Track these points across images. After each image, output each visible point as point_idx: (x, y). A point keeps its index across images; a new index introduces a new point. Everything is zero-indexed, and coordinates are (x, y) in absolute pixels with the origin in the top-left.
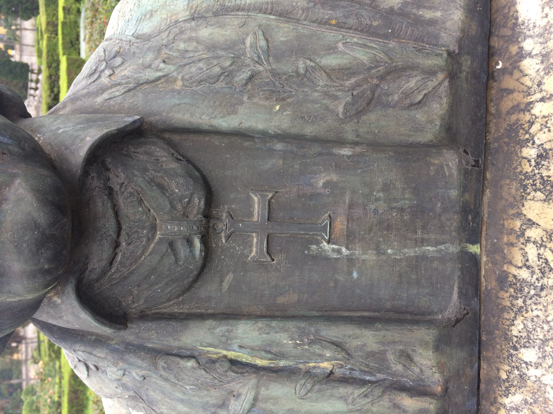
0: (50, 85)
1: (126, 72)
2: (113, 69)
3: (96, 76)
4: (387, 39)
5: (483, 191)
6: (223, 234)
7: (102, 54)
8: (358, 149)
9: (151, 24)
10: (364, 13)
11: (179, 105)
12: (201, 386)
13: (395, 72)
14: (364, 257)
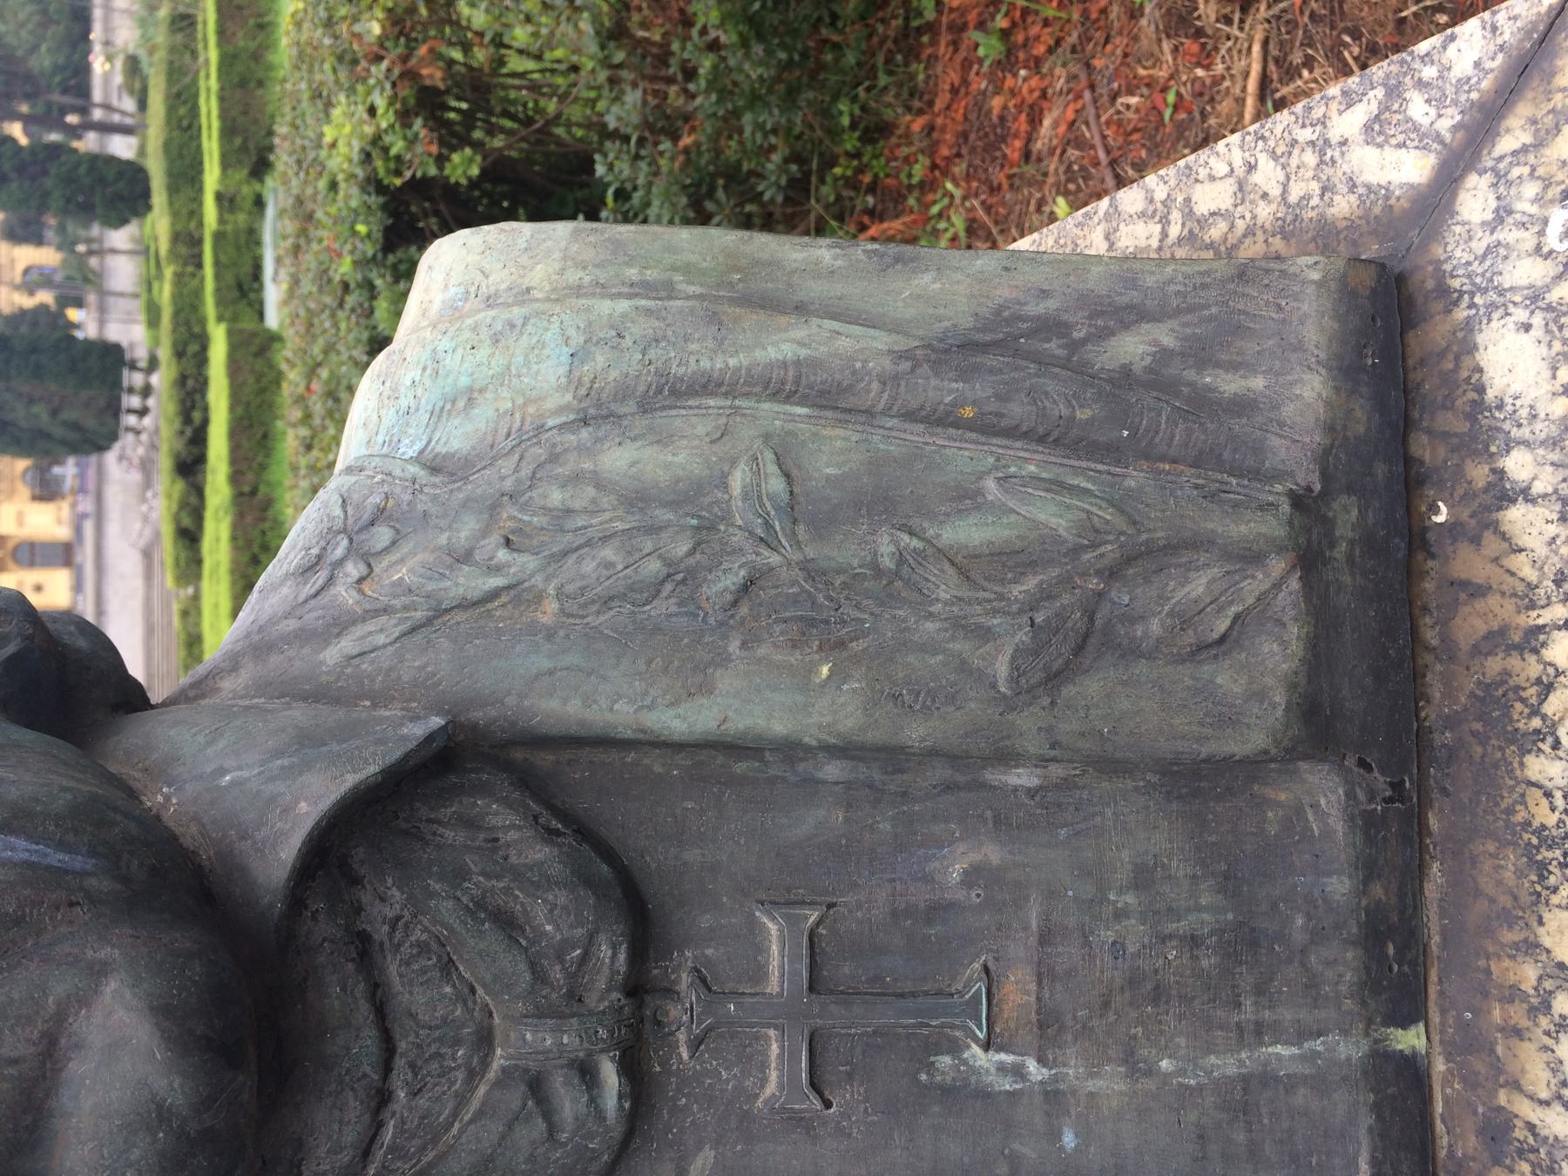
0: (182, 402)
1: (401, 573)
2: (368, 559)
3: (321, 577)
4: (1118, 463)
5: (1422, 871)
6: (682, 1036)
7: (338, 512)
8: (1057, 771)
9: (469, 428)
10: (1051, 386)
11: (551, 673)
13: (1147, 557)
14: (1092, 1085)
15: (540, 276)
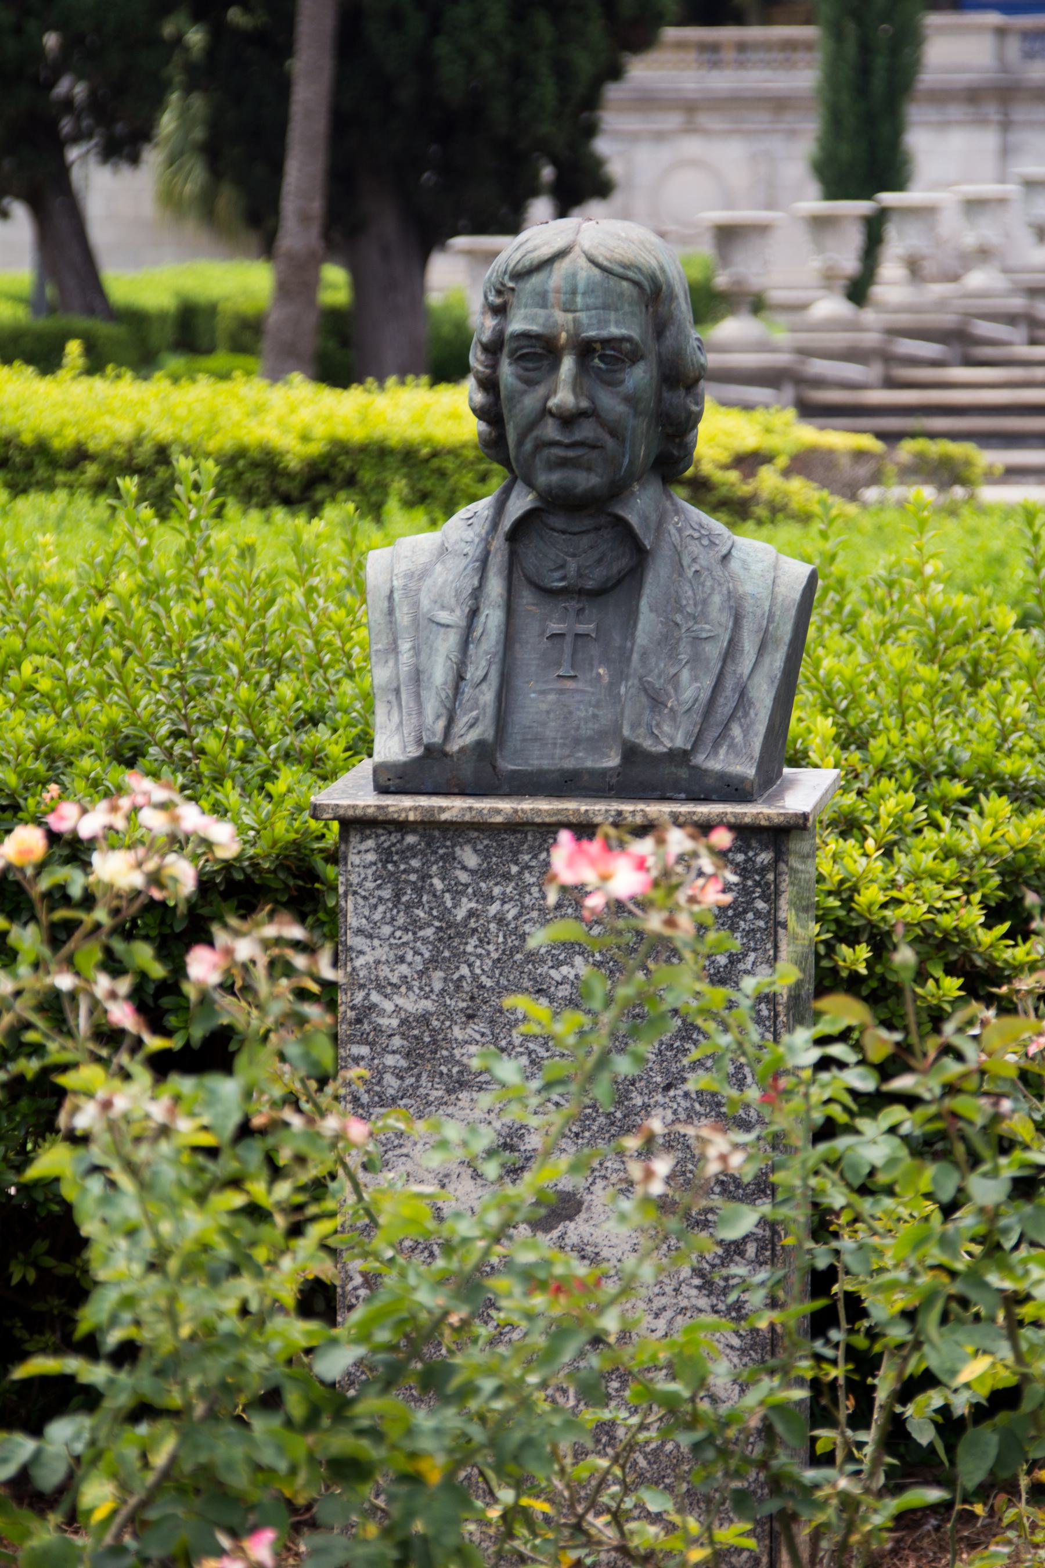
12: (458, 594)
15: (781, 590)
